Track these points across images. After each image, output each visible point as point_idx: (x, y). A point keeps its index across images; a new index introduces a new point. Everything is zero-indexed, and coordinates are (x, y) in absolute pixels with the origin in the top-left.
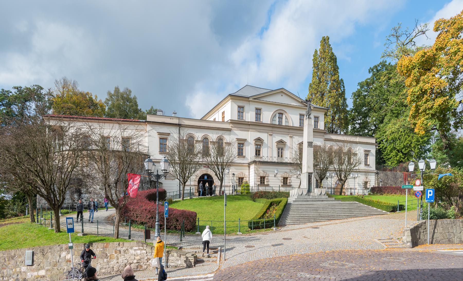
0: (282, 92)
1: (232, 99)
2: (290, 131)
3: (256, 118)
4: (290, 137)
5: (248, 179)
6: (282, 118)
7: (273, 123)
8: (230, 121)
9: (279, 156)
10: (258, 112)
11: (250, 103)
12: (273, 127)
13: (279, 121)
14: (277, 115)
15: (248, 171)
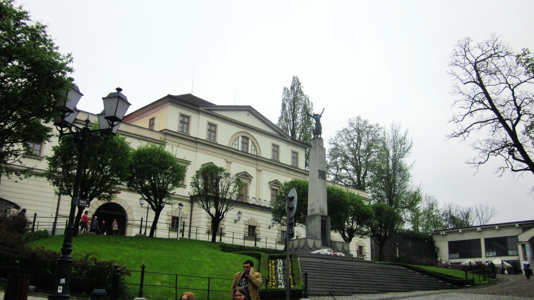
0: (248, 111)
1: (170, 101)
2: (259, 163)
3: (210, 136)
4: (258, 170)
5: (187, 221)
6: (247, 144)
7: (233, 147)
8: (165, 132)
9: (240, 196)
10: (212, 129)
11: (200, 113)
12: (233, 153)
13: (242, 147)
14: (240, 139)
15: (190, 209)
